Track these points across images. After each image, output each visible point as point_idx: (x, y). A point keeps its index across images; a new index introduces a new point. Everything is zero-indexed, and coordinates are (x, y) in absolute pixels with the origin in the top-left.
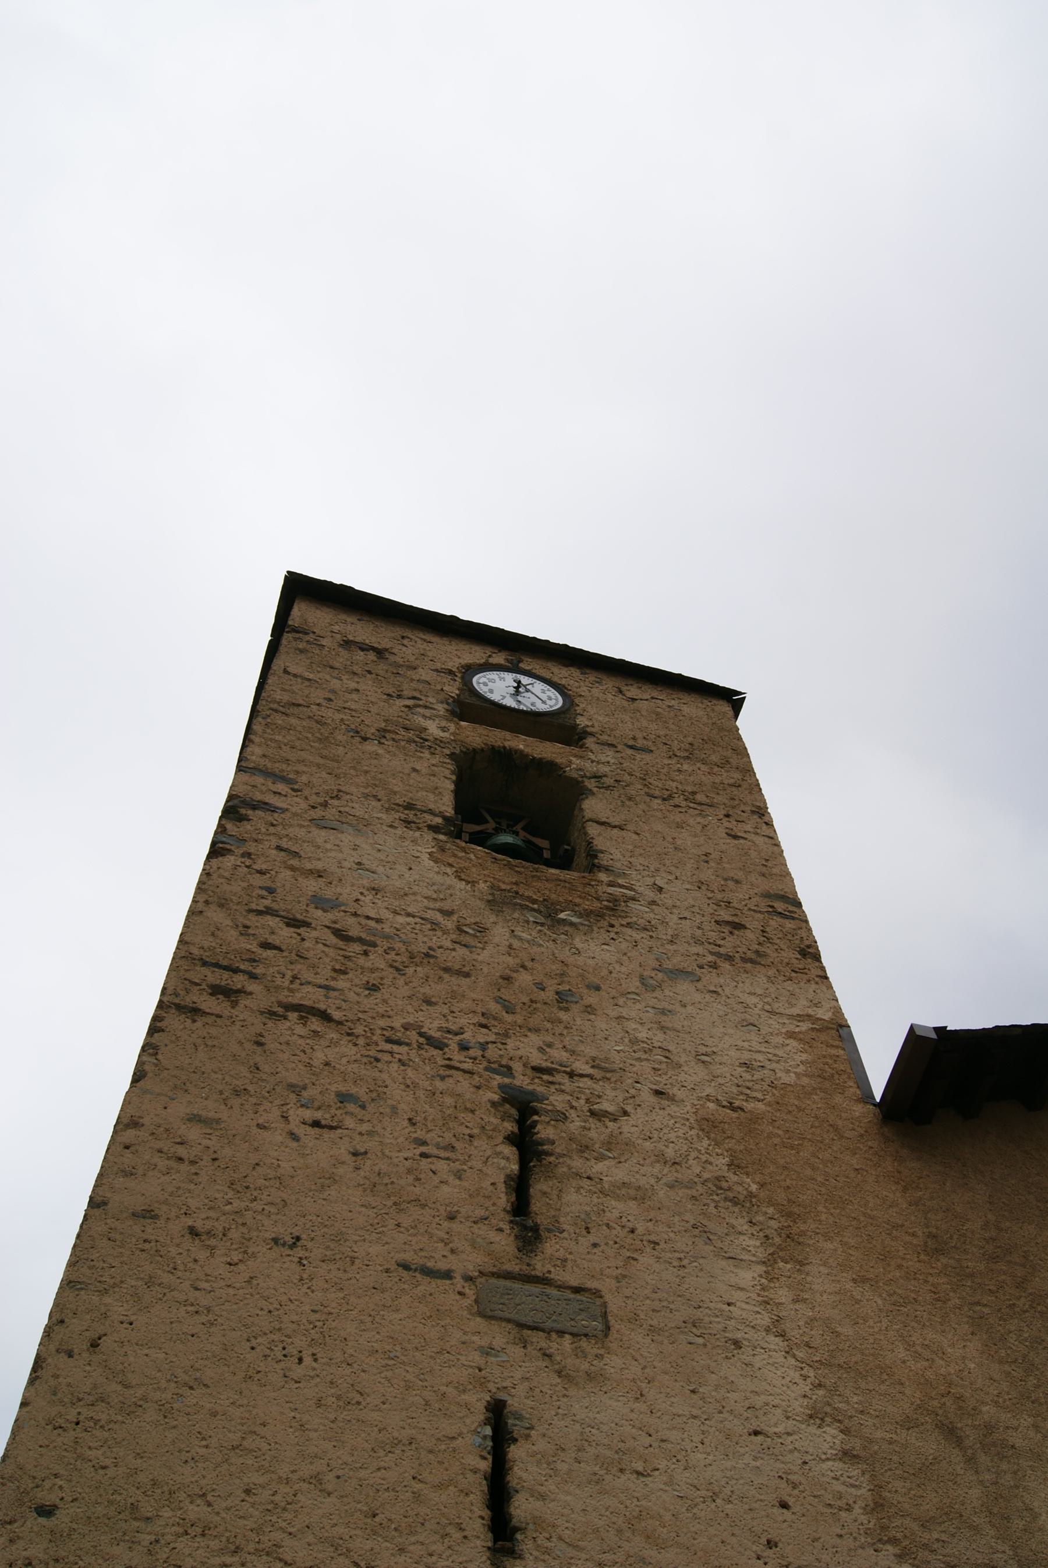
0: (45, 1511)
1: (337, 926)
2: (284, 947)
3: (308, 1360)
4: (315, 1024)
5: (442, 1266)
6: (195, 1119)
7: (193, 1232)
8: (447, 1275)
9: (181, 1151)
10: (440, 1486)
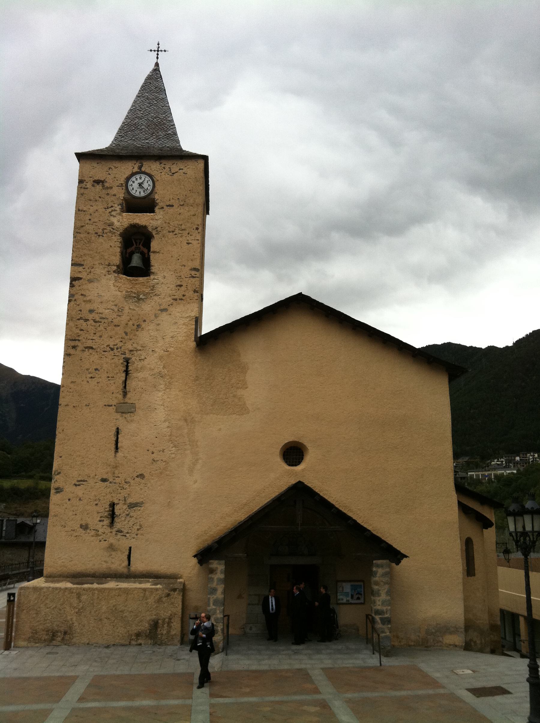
0: (61, 457)
1: (94, 318)
3: (91, 427)
4: (91, 351)
5: (111, 404)
6: (72, 382)
7: (74, 407)
8: (111, 406)
9: (71, 390)
10: (109, 443)
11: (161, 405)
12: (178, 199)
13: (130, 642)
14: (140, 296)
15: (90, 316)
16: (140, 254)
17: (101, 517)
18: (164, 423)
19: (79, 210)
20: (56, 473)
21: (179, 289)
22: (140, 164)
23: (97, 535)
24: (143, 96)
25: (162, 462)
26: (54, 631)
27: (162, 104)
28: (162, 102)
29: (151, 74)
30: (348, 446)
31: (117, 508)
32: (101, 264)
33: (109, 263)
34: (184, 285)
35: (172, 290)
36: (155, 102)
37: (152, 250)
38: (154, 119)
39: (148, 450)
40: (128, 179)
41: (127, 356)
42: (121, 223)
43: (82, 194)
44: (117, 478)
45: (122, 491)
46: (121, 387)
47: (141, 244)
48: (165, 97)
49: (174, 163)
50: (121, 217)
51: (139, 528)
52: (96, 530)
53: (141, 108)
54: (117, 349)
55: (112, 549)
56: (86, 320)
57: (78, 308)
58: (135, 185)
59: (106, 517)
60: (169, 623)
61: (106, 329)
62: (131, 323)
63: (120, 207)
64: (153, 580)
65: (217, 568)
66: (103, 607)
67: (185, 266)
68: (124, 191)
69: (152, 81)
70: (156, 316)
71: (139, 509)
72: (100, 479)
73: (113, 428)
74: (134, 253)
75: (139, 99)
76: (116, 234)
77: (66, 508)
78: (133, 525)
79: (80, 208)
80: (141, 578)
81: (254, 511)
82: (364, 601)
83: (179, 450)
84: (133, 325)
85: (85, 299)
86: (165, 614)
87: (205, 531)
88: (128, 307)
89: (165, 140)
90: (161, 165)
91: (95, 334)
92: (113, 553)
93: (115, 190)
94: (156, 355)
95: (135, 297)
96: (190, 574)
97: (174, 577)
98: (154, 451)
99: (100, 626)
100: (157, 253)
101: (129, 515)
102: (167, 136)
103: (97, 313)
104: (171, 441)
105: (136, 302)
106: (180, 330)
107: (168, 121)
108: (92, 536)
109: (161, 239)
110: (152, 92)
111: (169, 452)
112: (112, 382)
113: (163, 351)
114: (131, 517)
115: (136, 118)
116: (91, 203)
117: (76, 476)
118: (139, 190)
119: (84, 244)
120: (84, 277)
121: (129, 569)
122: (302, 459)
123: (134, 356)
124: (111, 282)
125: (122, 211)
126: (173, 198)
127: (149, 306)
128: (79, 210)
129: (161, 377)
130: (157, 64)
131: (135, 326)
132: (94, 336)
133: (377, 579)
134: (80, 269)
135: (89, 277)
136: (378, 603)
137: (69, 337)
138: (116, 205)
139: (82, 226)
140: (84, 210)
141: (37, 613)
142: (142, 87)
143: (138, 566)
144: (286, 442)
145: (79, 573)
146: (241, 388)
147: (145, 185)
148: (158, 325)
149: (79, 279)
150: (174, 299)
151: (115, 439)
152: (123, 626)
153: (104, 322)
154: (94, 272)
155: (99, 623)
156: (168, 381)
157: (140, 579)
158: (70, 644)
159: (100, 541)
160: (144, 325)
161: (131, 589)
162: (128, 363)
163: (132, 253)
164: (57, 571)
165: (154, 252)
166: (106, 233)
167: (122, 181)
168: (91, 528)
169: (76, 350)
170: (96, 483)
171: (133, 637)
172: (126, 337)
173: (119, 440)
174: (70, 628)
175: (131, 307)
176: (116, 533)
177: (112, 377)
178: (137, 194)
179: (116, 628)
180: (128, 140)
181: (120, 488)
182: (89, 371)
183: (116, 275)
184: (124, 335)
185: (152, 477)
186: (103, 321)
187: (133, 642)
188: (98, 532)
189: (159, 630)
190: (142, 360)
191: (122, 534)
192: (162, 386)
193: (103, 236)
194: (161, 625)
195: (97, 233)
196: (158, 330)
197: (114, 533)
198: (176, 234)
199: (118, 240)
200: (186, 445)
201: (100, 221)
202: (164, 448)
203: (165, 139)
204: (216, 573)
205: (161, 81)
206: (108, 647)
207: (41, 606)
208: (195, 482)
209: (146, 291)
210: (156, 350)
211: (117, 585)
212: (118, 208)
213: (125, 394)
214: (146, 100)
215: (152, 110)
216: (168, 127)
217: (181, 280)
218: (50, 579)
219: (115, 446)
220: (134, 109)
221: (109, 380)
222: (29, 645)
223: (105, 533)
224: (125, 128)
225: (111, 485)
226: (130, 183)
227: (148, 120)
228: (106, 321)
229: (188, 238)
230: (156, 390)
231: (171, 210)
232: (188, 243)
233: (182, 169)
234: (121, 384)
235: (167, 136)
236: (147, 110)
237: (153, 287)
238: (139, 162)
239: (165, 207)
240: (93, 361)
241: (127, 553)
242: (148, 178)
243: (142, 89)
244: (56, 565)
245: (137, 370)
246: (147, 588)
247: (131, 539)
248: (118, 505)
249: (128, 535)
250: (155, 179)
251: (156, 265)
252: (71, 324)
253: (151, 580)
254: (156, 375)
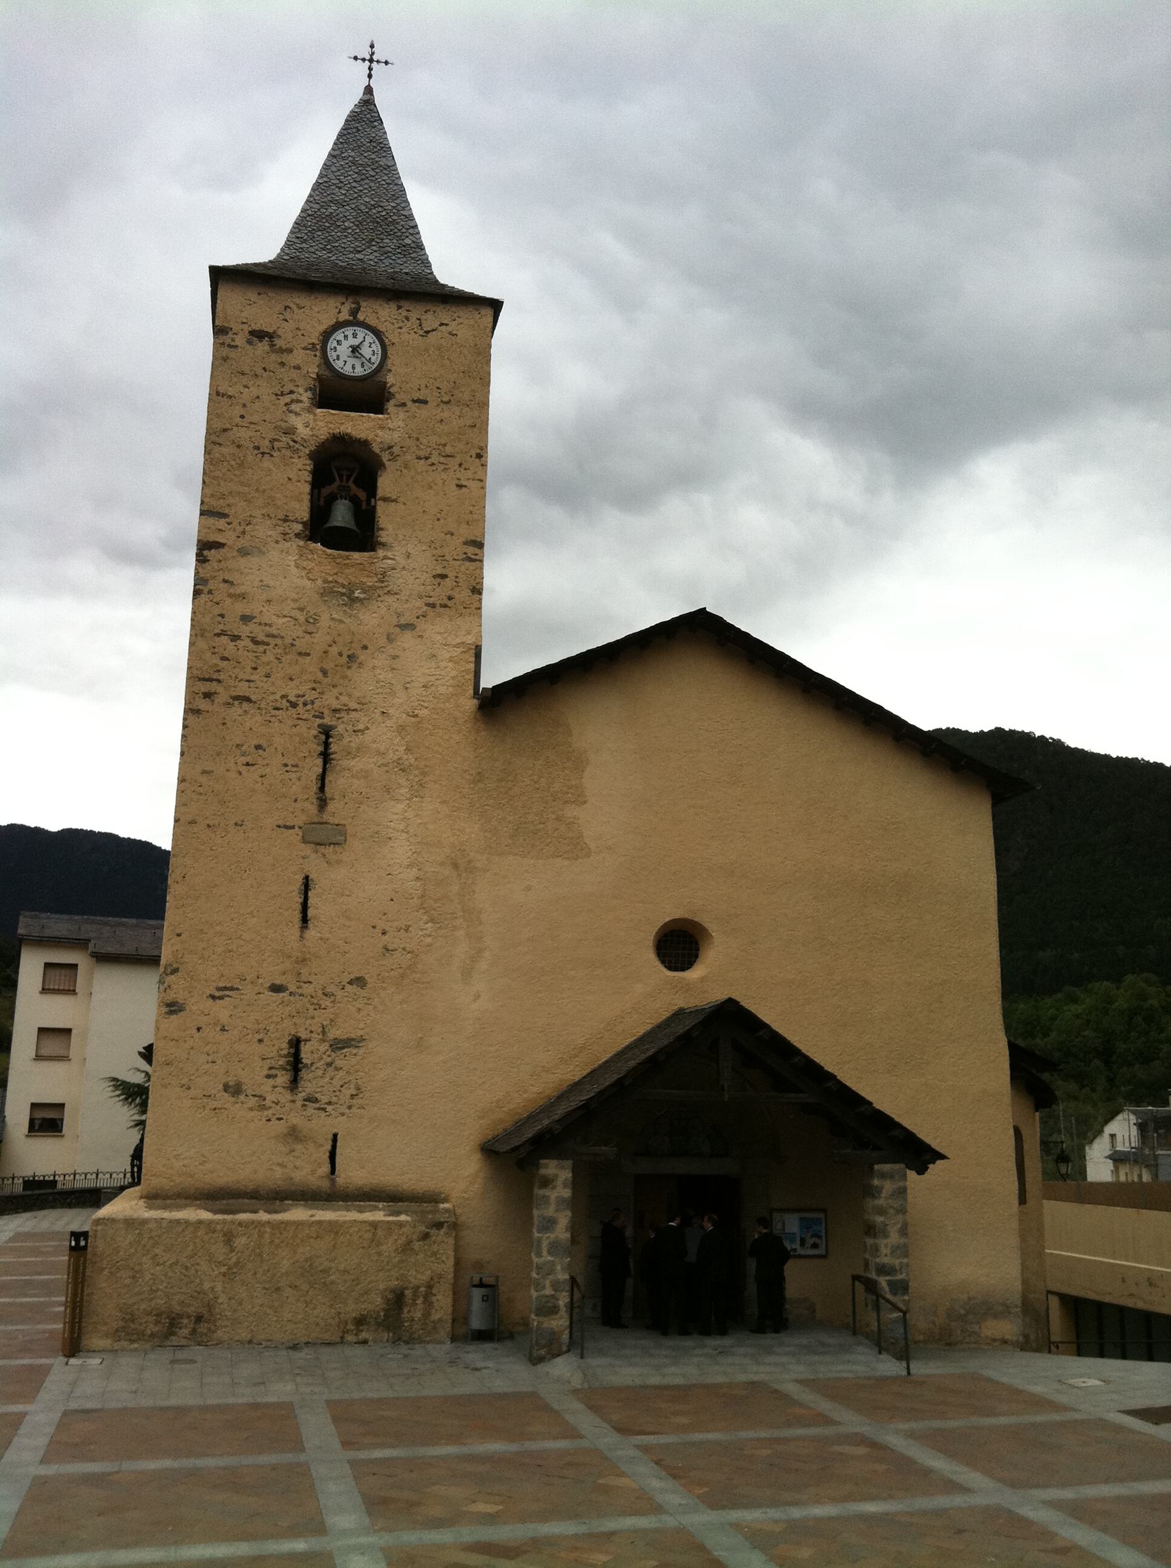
0: (179, 935)
2: (230, 658)
4: (245, 704)
6: (204, 772)
7: (209, 826)
8: (293, 827)
9: (201, 790)
11: (403, 831)
12: (438, 388)
13: (342, 1338)
14: (354, 593)
15: (245, 630)
16: (350, 501)
17: (271, 1068)
18: (408, 870)
19: (218, 394)
20: (169, 971)
21: (439, 584)
22: (353, 306)
23: (263, 1108)
24: (343, 155)
25: (404, 952)
26: (173, 1315)
27: (385, 178)
28: (386, 174)
29: (356, 110)
30: (793, 932)
31: (305, 1050)
32: (268, 515)
33: (286, 516)
34: (452, 574)
35: (423, 585)
36: (372, 173)
37: (380, 493)
38: (371, 209)
39: (374, 927)
40: (327, 335)
41: (327, 721)
42: (312, 429)
43: (225, 359)
44: (307, 985)
45: (316, 1013)
46: (315, 788)
47: (352, 479)
48: (393, 164)
49: (429, 310)
50: (311, 417)
51: (354, 1093)
52: (260, 1096)
53: (342, 182)
54: (305, 704)
55: (296, 1138)
56: (235, 638)
57: (217, 610)
58: (344, 350)
59: (283, 1068)
60: (427, 1296)
61: (279, 659)
62: (334, 650)
63: (309, 394)
64: (385, 1204)
65: (556, 1176)
66: (285, 1262)
67: (452, 534)
68: (317, 361)
69: (361, 126)
70: (390, 639)
71: (354, 1051)
72: (268, 985)
73: (297, 877)
74: (337, 499)
75: (335, 161)
76: (301, 454)
77: (192, 1048)
78: (342, 1086)
79: (221, 390)
80: (360, 1201)
81: (600, 1062)
82: (827, 1252)
83: (440, 928)
84: (340, 654)
85: (232, 591)
86: (419, 1276)
87: (498, 1101)
88: (329, 614)
89: (399, 258)
90: (400, 311)
91: (255, 669)
92: (299, 1147)
93: (298, 357)
94: (389, 723)
95: (343, 594)
96: (465, 1192)
97: (432, 1199)
98: (387, 929)
99: (276, 1304)
100: (392, 501)
101: (334, 1065)
102: (403, 248)
103: (260, 624)
104: (424, 908)
105: (345, 605)
106: (442, 673)
107: (402, 217)
108: (251, 1109)
109: (401, 471)
110: (362, 149)
111: (421, 933)
112: (293, 776)
113: (404, 716)
114: (337, 1069)
115: (331, 201)
116: (244, 380)
117: (213, 978)
118: (351, 361)
119: (229, 470)
120: (229, 543)
121: (333, 1181)
122: (697, 956)
123: (343, 722)
124: (290, 557)
125: (314, 405)
126: (426, 386)
127: (374, 615)
128: (218, 394)
129: (400, 769)
130: (369, 90)
131: (345, 659)
132: (252, 674)
133: (881, 1202)
134: (221, 523)
135: (242, 542)
136: (884, 1251)
137: (195, 672)
138: (301, 390)
139: (225, 430)
140: (229, 394)
141: (134, 1277)
142: (340, 135)
143: (352, 1174)
144: (667, 920)
145: (221, 1189)
146: (573, 802)
147: (366, 351)
148: (395, 657)
149: (218, 545)
150: (428, 605)
151: (301, 900)
152: (328, 1304)
153: (276, 645)
154: (252, 534)
155: (275, 1296)
156: (417, 779)
157: (358, 1203)
159: (269, 1120)
160: (362, 656)
161: (345, 1222)
162: (328, 736)
163: (332, 499)
165: (385, 499)
166: (279, 450)
167: (314, 338)
168: (249, 1092)
169: (213, 701)
170: (259, 993)
171: (350, 1327)
172: (325, 681)
173: (310, 901)
174: (210, 1307)
175: (335, 616)
176: (301, 1103)
177: (293, 766)
178: (347, 370)
179: (311, 1306)
180: (317, 250)
181: (313, 1007)
182: (243, 748)
183: (302, 543)
184: (320, 675)
185: (384, 985)
186: (272, 641)
187: (350, 1338)
188: (265, 1100)
189: (405, 1311)
190: (359, 731)
191: (317, 1105)
192: (403, 791)
193: (272, 456)
194: (410, 1301)
195: (257, 448)
196: (394, 669)
197: (299, 1103)
198: (433, 464)
199: (305, 467)
200: (456, 918)
201: (265, 421)
202: (409, 923)
203: (399, 256)
204: (554, 1188)
205: (380, 127)
206: (295, 1347)
207: (144, 1259)
208: (477, 997)
209: (369, 584)
210: (391, 711)
211: (312, 1216)
212: (306, 397)
213: (323, 803)
214: (350, 166)
215: (366, 189)
216: (404, 230)
217: (445, 563)
218: (159, 1202)
219: (301, 915)
220: (326, 182)
221: (287, 771)
222: (116, 1346)
223: (279, 1102)
224: (309, 224)
225: (292, 998)
226: (332, 343)
227: (359, 209)
228: (279, 641)
229: (459, 475)
230: (391, 799)
231: (423, 412)
232: (460, 486)
233: (447, 325)
234: (314, 781)
235: (403, 248)
236: (355, 187)
237: (384, 574)
238: (350, 300)
239: (409, 404)
240: (251, 729)
241: (329, 1147)
242: (370, 338)
243: (341, 140)
245: (349, 753)
246: (379, 1222)
247: (336, 1117)
248: (308, 1043)
249: (329, 1108)
250: (387, 340)
251: (390, 527)
252: (202, 644)
253: (381, 1205)
254: (391, 766)
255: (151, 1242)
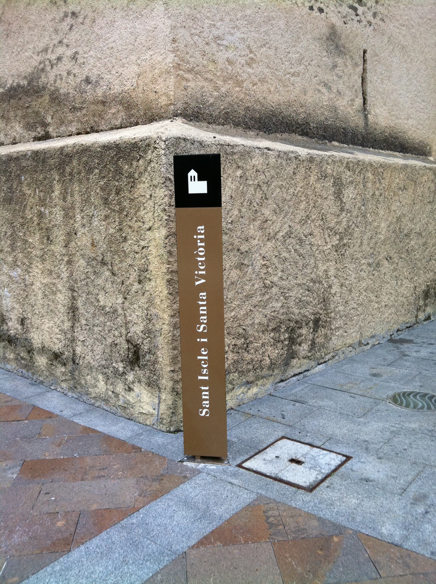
92: (340, 61)
121: (366, 117)
145: (274, 114)
158: (327, 357)
164: (216, 93)
244: (211, 67)
255: (259, 195)
